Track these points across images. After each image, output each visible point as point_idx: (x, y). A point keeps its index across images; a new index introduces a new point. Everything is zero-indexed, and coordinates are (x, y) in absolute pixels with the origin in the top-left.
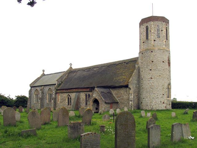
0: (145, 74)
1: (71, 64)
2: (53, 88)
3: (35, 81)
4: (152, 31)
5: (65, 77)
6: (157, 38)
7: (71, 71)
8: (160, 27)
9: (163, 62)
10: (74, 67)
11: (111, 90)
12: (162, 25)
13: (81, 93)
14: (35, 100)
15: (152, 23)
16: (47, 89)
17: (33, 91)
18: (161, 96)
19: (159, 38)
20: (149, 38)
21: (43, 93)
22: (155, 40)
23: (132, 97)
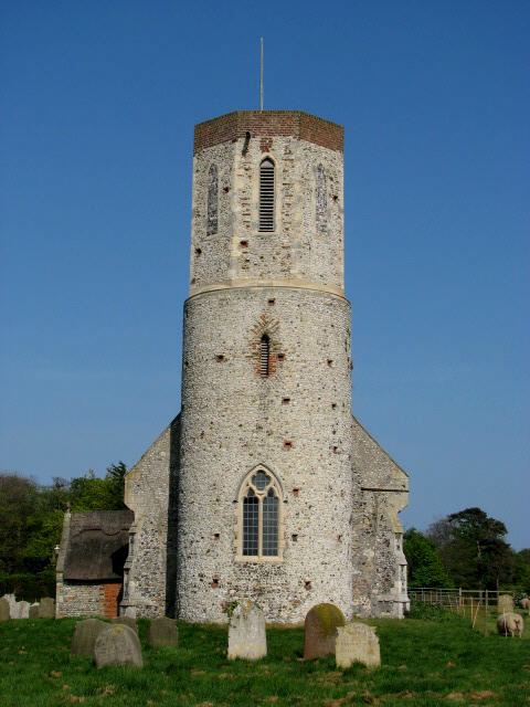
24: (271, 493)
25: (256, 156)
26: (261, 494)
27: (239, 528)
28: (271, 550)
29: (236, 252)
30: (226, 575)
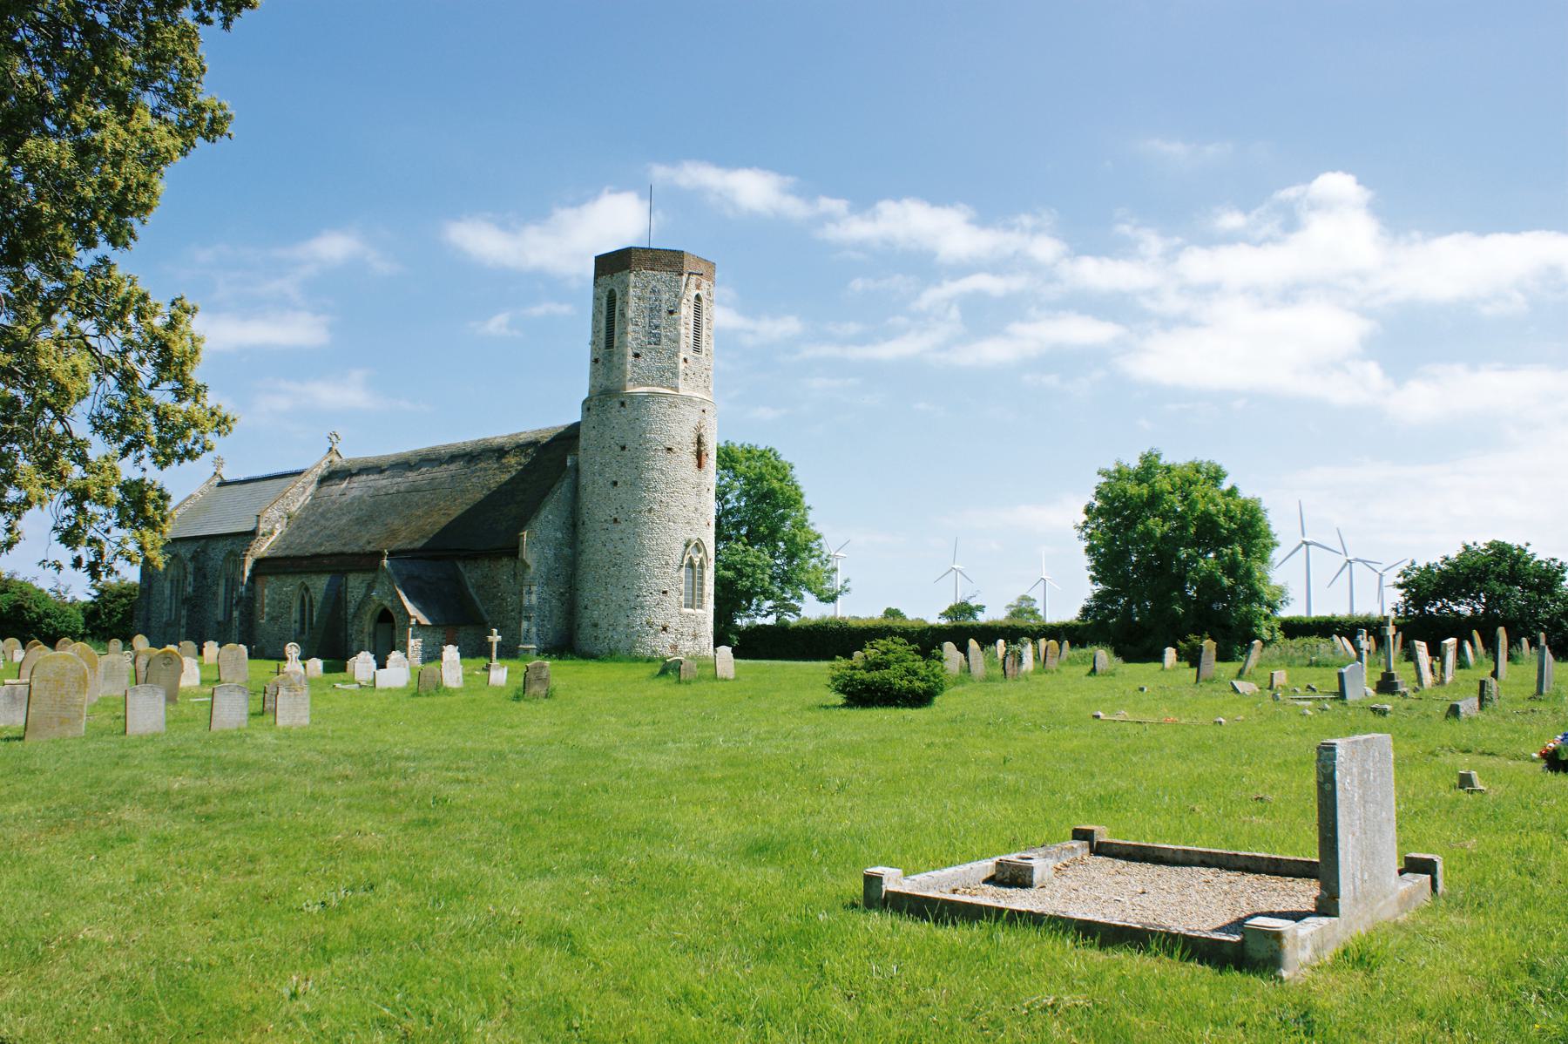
0: (597, 507)
4: (630, 314)
5: (302, 499)
8: (665, 297)
11: (460, 565)
14: (166, 606)
20: (616, 343)
26: (697, 561)
27: (682, 586)
28: (700, 607)
29: (682, 366)
30: (674, 623)
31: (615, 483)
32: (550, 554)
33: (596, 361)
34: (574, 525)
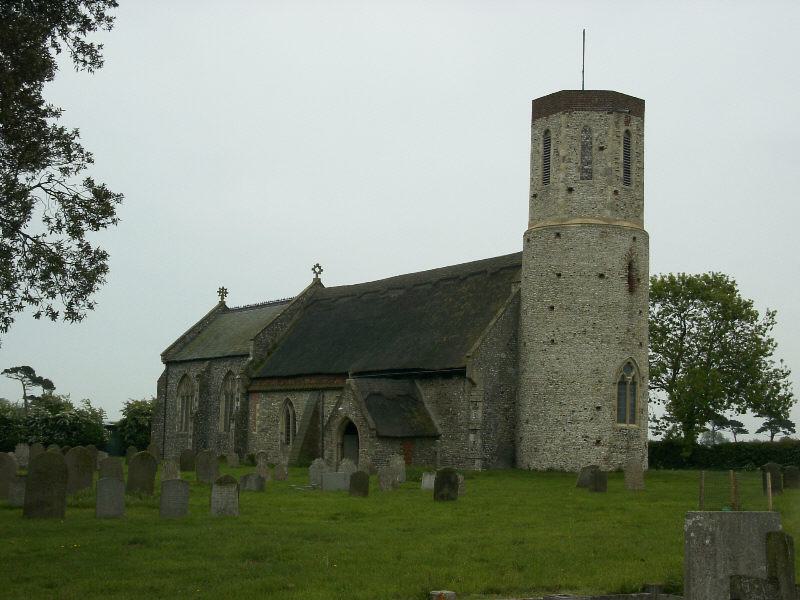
0: (536, 328)
1: (318, 269)
2: (237, 369)
3: (183, 338)
4: (562, 152)
6: (582, 178)
7: (317, 299)
9: (602, 276)
10: (329, 281)
11: (418, 383)
12: (605, 128)
13: (327, 394)
15: (563, 118)
16: (219, 372)
17: (173, 382)
18: (587, 414)
19: (591, 177)
21: (205, 388)
22: (570, 190)
23: (477, 415)
24: (633, 377)
25: (623, 129)
28: (633, 421)
30: (607, 438)
31: (552, 308)
32: (495, 372)
33: (535, 196)
34: (514, 345)
